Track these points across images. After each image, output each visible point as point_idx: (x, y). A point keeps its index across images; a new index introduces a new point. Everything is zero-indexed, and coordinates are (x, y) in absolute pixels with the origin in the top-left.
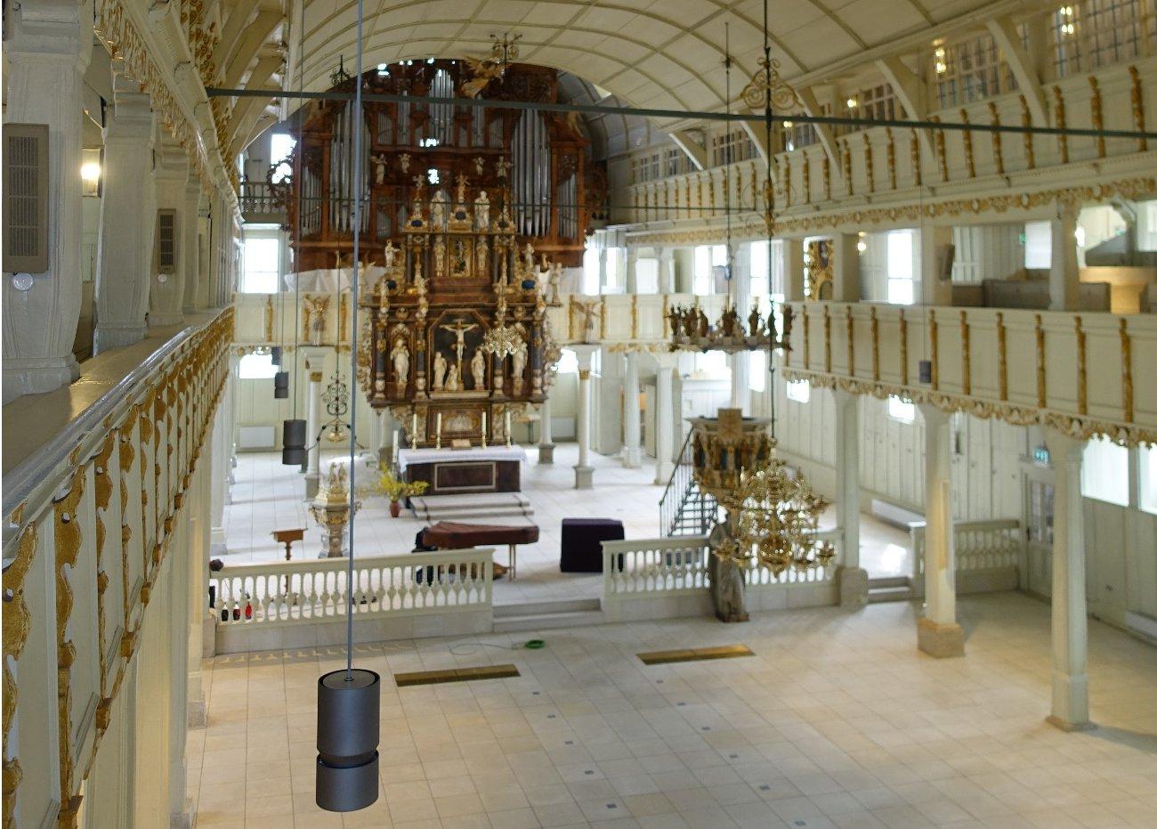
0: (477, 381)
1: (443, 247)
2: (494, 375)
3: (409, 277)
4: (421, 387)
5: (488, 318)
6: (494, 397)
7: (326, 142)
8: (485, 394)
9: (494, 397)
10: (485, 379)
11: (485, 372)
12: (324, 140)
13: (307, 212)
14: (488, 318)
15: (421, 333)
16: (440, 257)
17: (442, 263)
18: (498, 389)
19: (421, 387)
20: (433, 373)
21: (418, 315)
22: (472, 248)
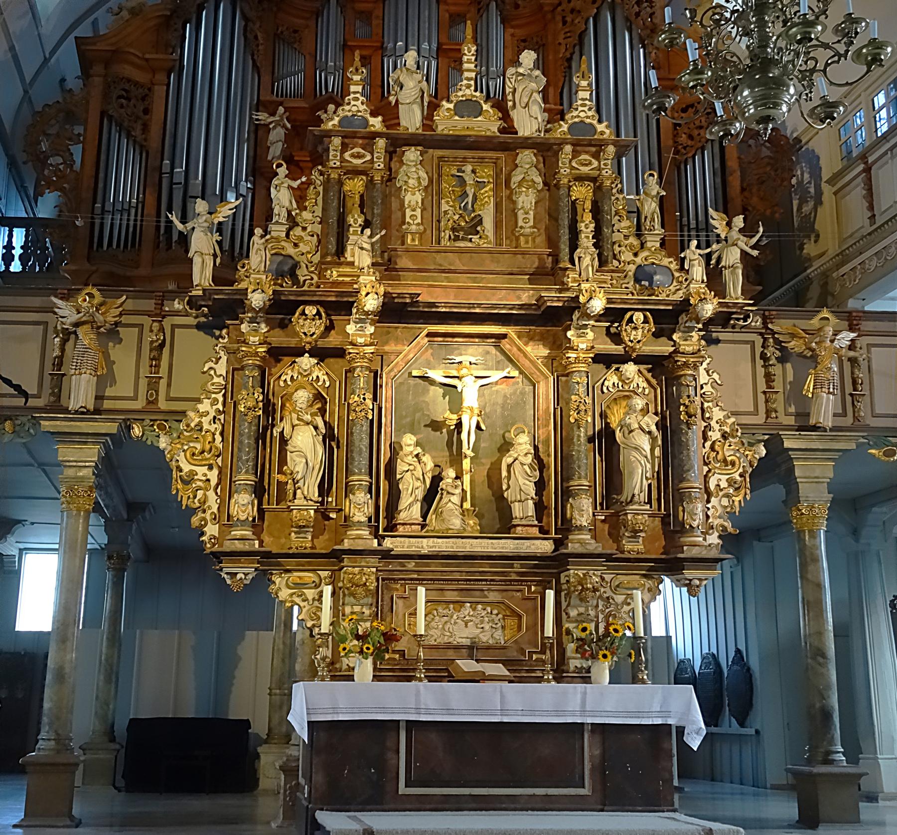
0: (517, 510)
1: (423, 174)
2: (566, 494)
3: (332, 248)
4: (360, 516)
5: (545, 352)
6: (572, 547)
7: (161, 77)
8: (546, 547)
9: (572, 547)
10: (540, 508)
11: (540, 485)
12: (154, 71)
13: (108, 207)
14: (545, 352)
15: (362, 380)
16: (413, 199)
17: (418, 212)
18: (580, 528)
19: (360, 516)
20: (394, 495)
21: (351, 328)
22: (497, 185)
